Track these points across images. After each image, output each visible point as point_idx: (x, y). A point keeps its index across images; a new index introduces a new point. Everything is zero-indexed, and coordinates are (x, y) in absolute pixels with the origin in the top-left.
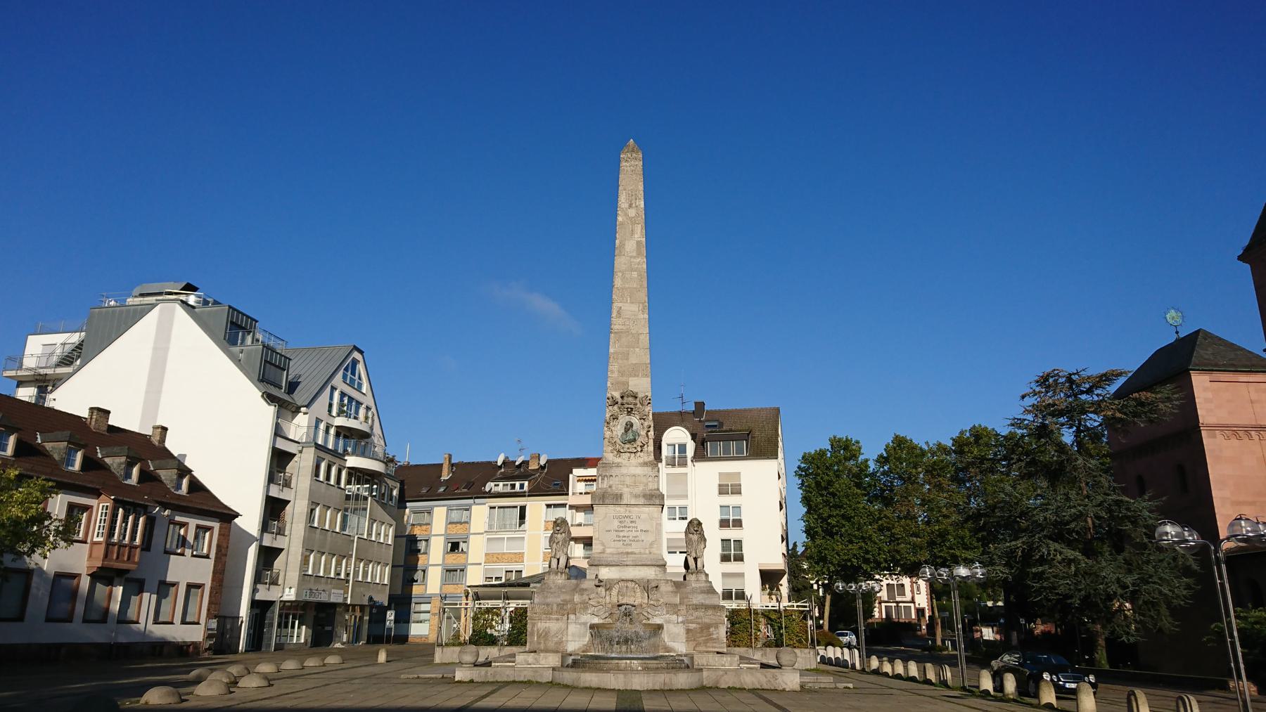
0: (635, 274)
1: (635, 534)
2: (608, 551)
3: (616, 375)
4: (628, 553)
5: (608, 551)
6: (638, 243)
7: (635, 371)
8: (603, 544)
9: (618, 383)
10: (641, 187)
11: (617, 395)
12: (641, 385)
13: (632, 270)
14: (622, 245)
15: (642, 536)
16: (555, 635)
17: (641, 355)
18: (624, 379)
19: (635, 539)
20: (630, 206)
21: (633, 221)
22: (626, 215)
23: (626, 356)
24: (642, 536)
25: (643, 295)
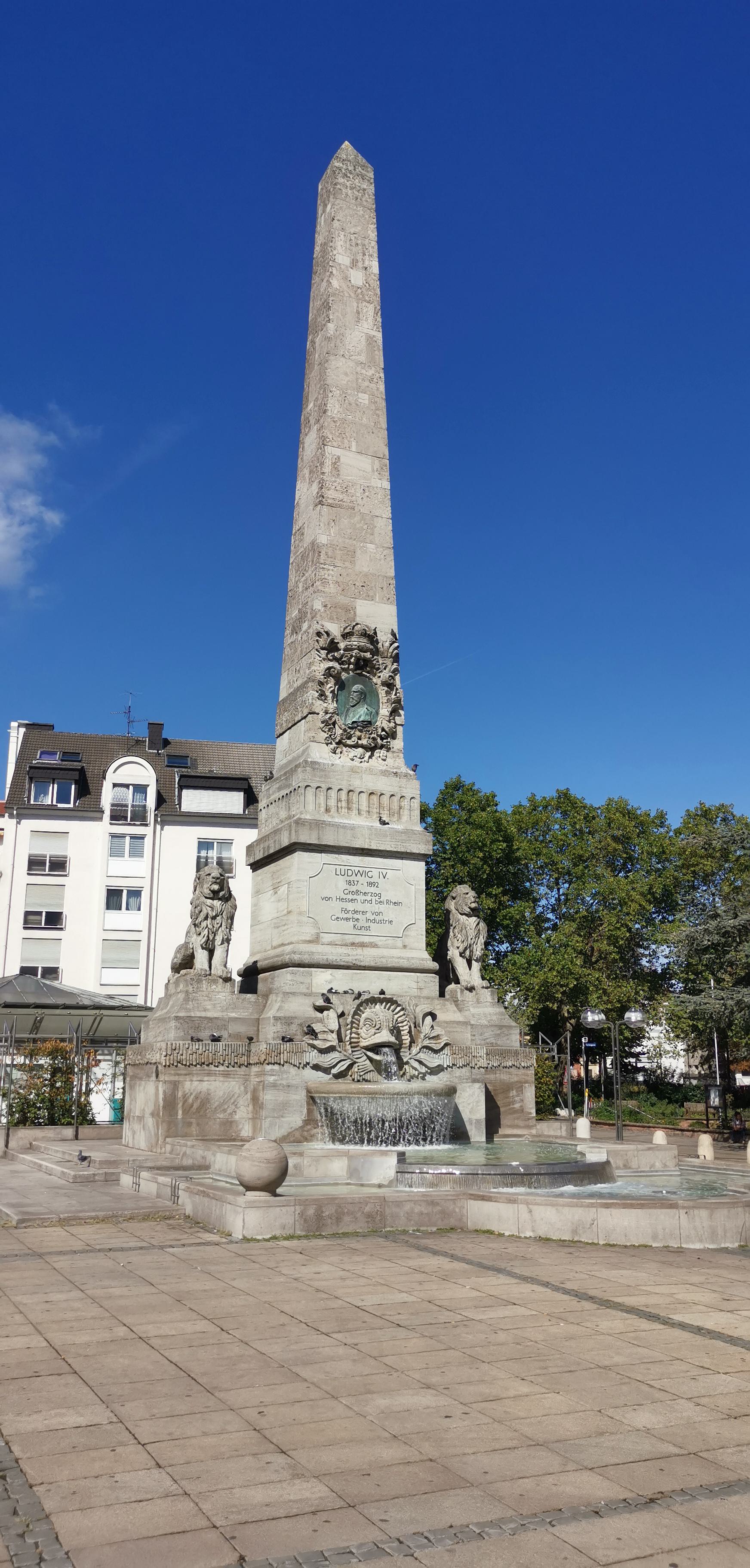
0: (364, 399)
1: (376, 908)
2: (326, 938)
3: (332, 589)
4: (362, 945)
5: (326, 938)
6: (370, 339)
7: (365, 590)
8: (316, 923)
9: (335, 606)
10: (373, 234)
11: (335, 630)
12: (381, 616)
13: (359, 389)
14: (340, 336)
15: (389, 913)
16: (222, 1107)
17: (377, 557)
18: (343, 600)
19: (378, 919)
20: (354, 263)
21: (359, 293)
22: (346, 278)
23: (351, 555)
24: (389, 913)
25: (380, 443)
